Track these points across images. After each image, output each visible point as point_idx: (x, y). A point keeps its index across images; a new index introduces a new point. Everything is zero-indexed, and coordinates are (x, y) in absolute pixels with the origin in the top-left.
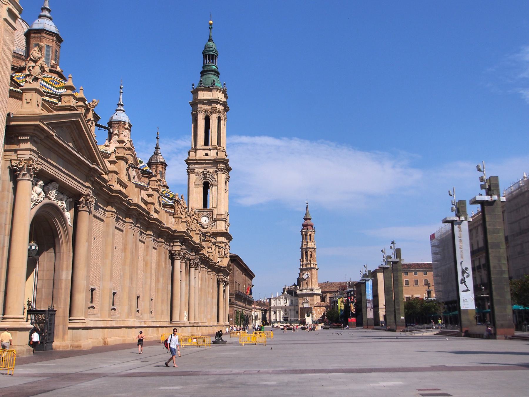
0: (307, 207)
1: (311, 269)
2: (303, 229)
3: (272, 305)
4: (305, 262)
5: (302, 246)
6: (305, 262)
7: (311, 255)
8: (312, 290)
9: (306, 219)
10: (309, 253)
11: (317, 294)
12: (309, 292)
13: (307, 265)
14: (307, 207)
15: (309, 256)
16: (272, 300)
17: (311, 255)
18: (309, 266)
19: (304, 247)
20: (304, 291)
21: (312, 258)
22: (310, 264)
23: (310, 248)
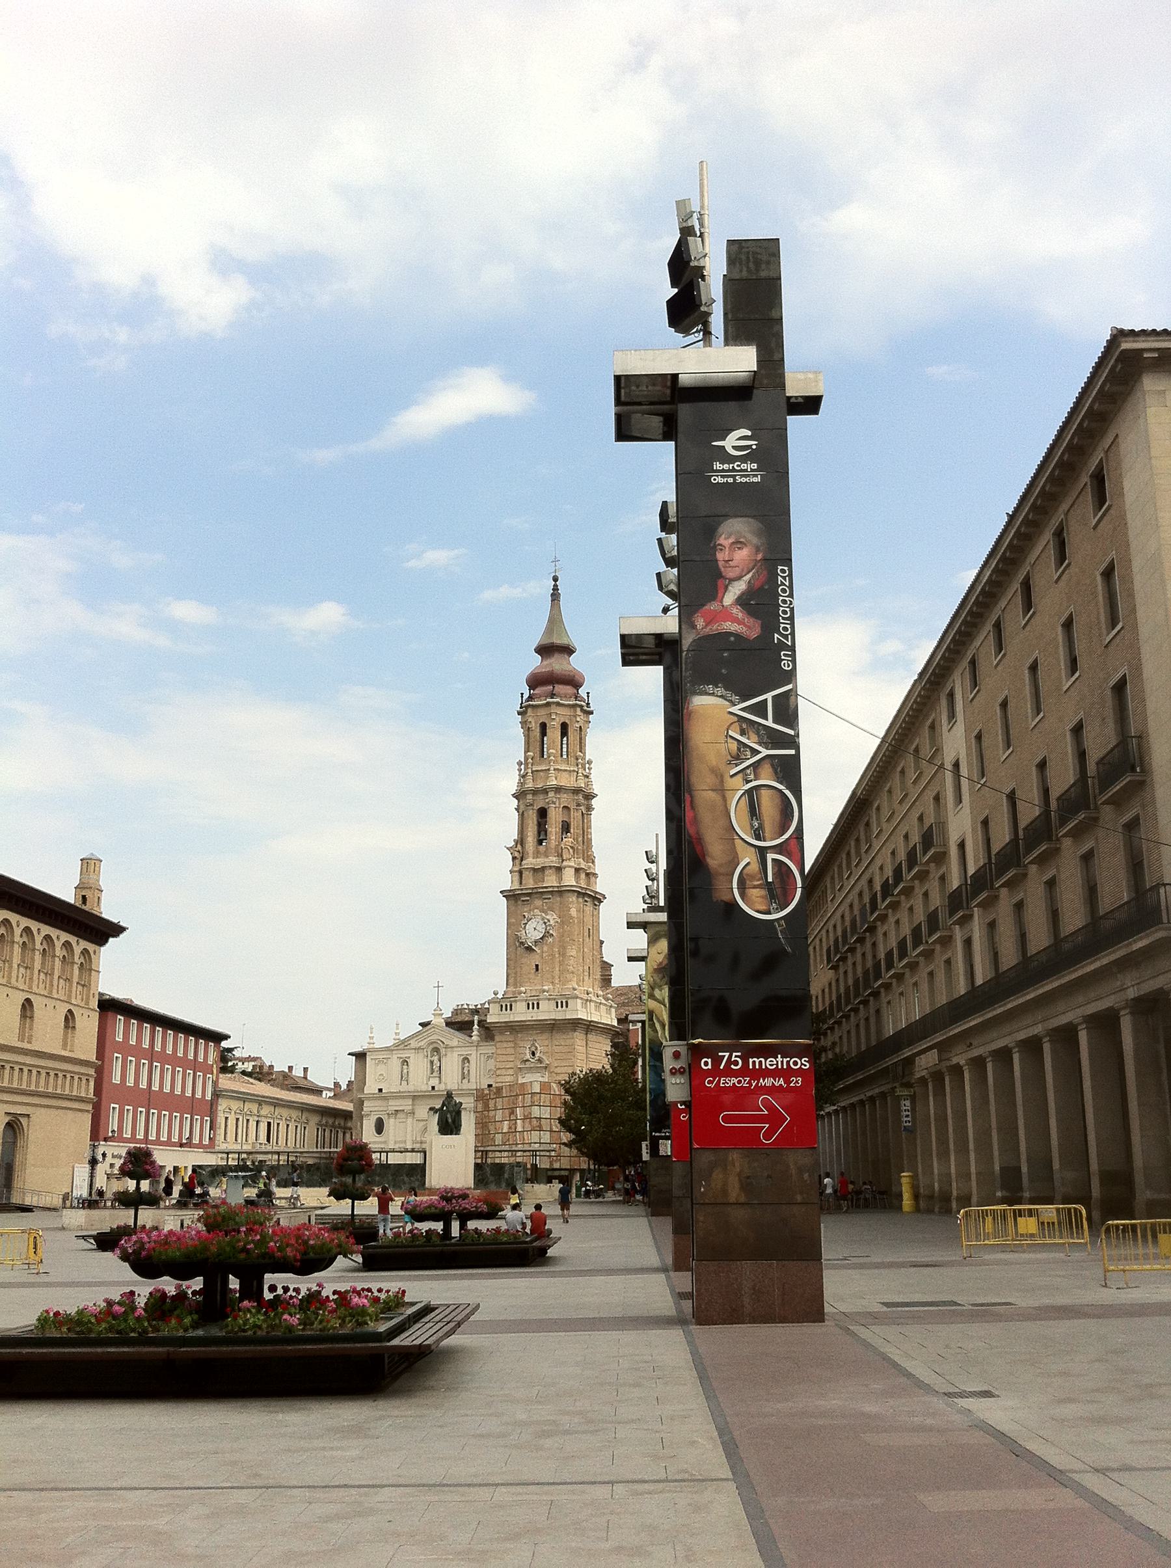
0: (555, 595)
1: (561, 892)
2: (530, 698)
3: (371, 1087)
4: (530, 862)
5: (521, 784)
6: (530, 862)
7: (566, 828)
8: (563, 1002)
9: (545, 650)
10: (555, 818)
11: (589, 1027)
12: (547, 1012)
13: (539, 871)
14: (555, 595)
15: (553, 829)
16: (368, 1058)
17: (566, 828)
18: (551, 881)
19: (530, 785)
20: (520, 1007)
21: (568, 840)
22: (559, 870)
23: (558, 789)
